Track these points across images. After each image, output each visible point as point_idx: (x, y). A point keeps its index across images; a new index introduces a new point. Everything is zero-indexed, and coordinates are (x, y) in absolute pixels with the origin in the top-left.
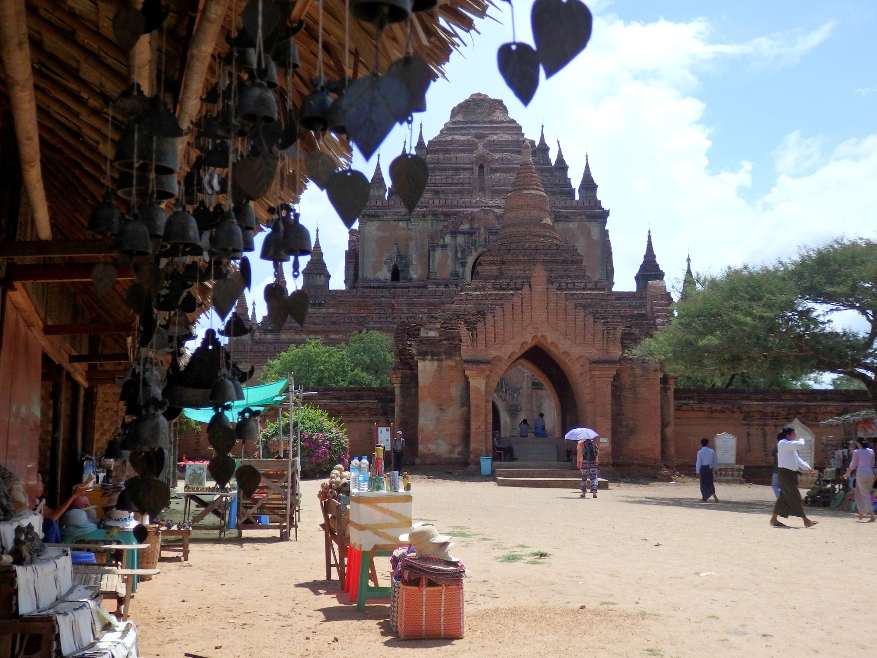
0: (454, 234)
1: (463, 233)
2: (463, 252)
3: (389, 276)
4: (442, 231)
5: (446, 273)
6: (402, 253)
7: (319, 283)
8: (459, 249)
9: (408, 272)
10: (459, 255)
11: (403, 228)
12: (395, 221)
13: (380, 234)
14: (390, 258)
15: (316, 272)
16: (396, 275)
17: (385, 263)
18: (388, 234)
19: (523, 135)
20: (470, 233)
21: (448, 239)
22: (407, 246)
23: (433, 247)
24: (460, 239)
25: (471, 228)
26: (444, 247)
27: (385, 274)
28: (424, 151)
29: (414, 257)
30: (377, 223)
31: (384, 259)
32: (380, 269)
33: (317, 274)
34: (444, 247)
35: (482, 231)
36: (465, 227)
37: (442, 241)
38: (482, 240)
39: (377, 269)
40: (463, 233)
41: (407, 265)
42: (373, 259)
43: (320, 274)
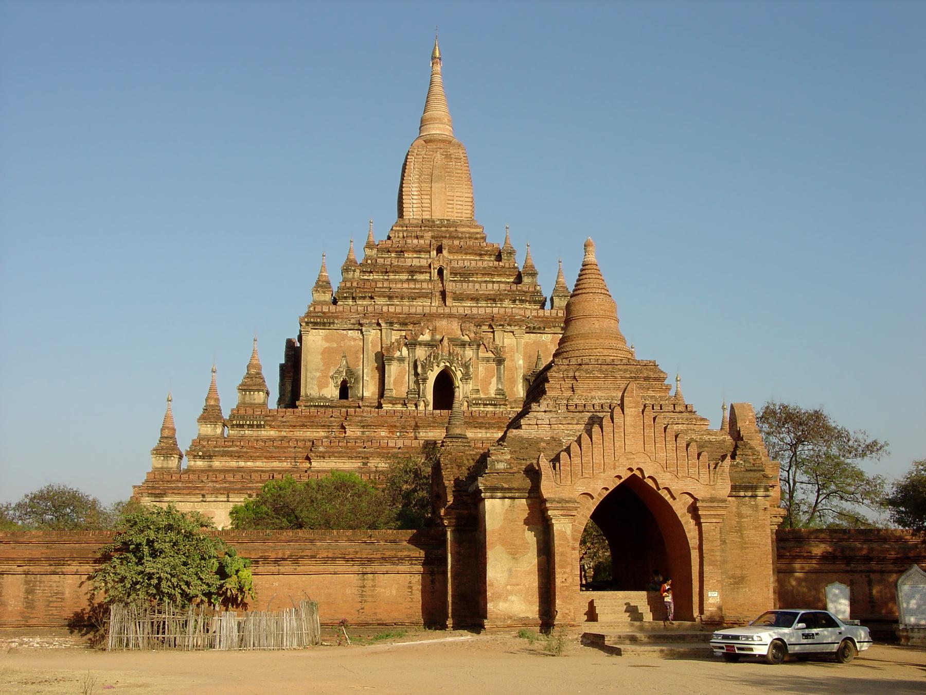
0: (412, 345)
2: (423, 367)
3: (336, 393)
4: (397, 340)
5: (402, 391)
6: (352, 367)
7: (256, 401)
8: (418, 363)
10: (419, 370)
13: (326, 345)
15: (254, 388)
16: (344, 391)
17: (332, 378)
19: (484, 238)
21: (405, 351)
24: (421, 353)
26: (401, 360)
27: (332, 392)
31: (331, 374)
32: (327, 385)
33: (254, 391)
34: (401, 360)
35: (445, 342)
36: (426, 337)
38: (446, 353)
39: (321, 386)
42: (318, 374)
43: (259, 391)
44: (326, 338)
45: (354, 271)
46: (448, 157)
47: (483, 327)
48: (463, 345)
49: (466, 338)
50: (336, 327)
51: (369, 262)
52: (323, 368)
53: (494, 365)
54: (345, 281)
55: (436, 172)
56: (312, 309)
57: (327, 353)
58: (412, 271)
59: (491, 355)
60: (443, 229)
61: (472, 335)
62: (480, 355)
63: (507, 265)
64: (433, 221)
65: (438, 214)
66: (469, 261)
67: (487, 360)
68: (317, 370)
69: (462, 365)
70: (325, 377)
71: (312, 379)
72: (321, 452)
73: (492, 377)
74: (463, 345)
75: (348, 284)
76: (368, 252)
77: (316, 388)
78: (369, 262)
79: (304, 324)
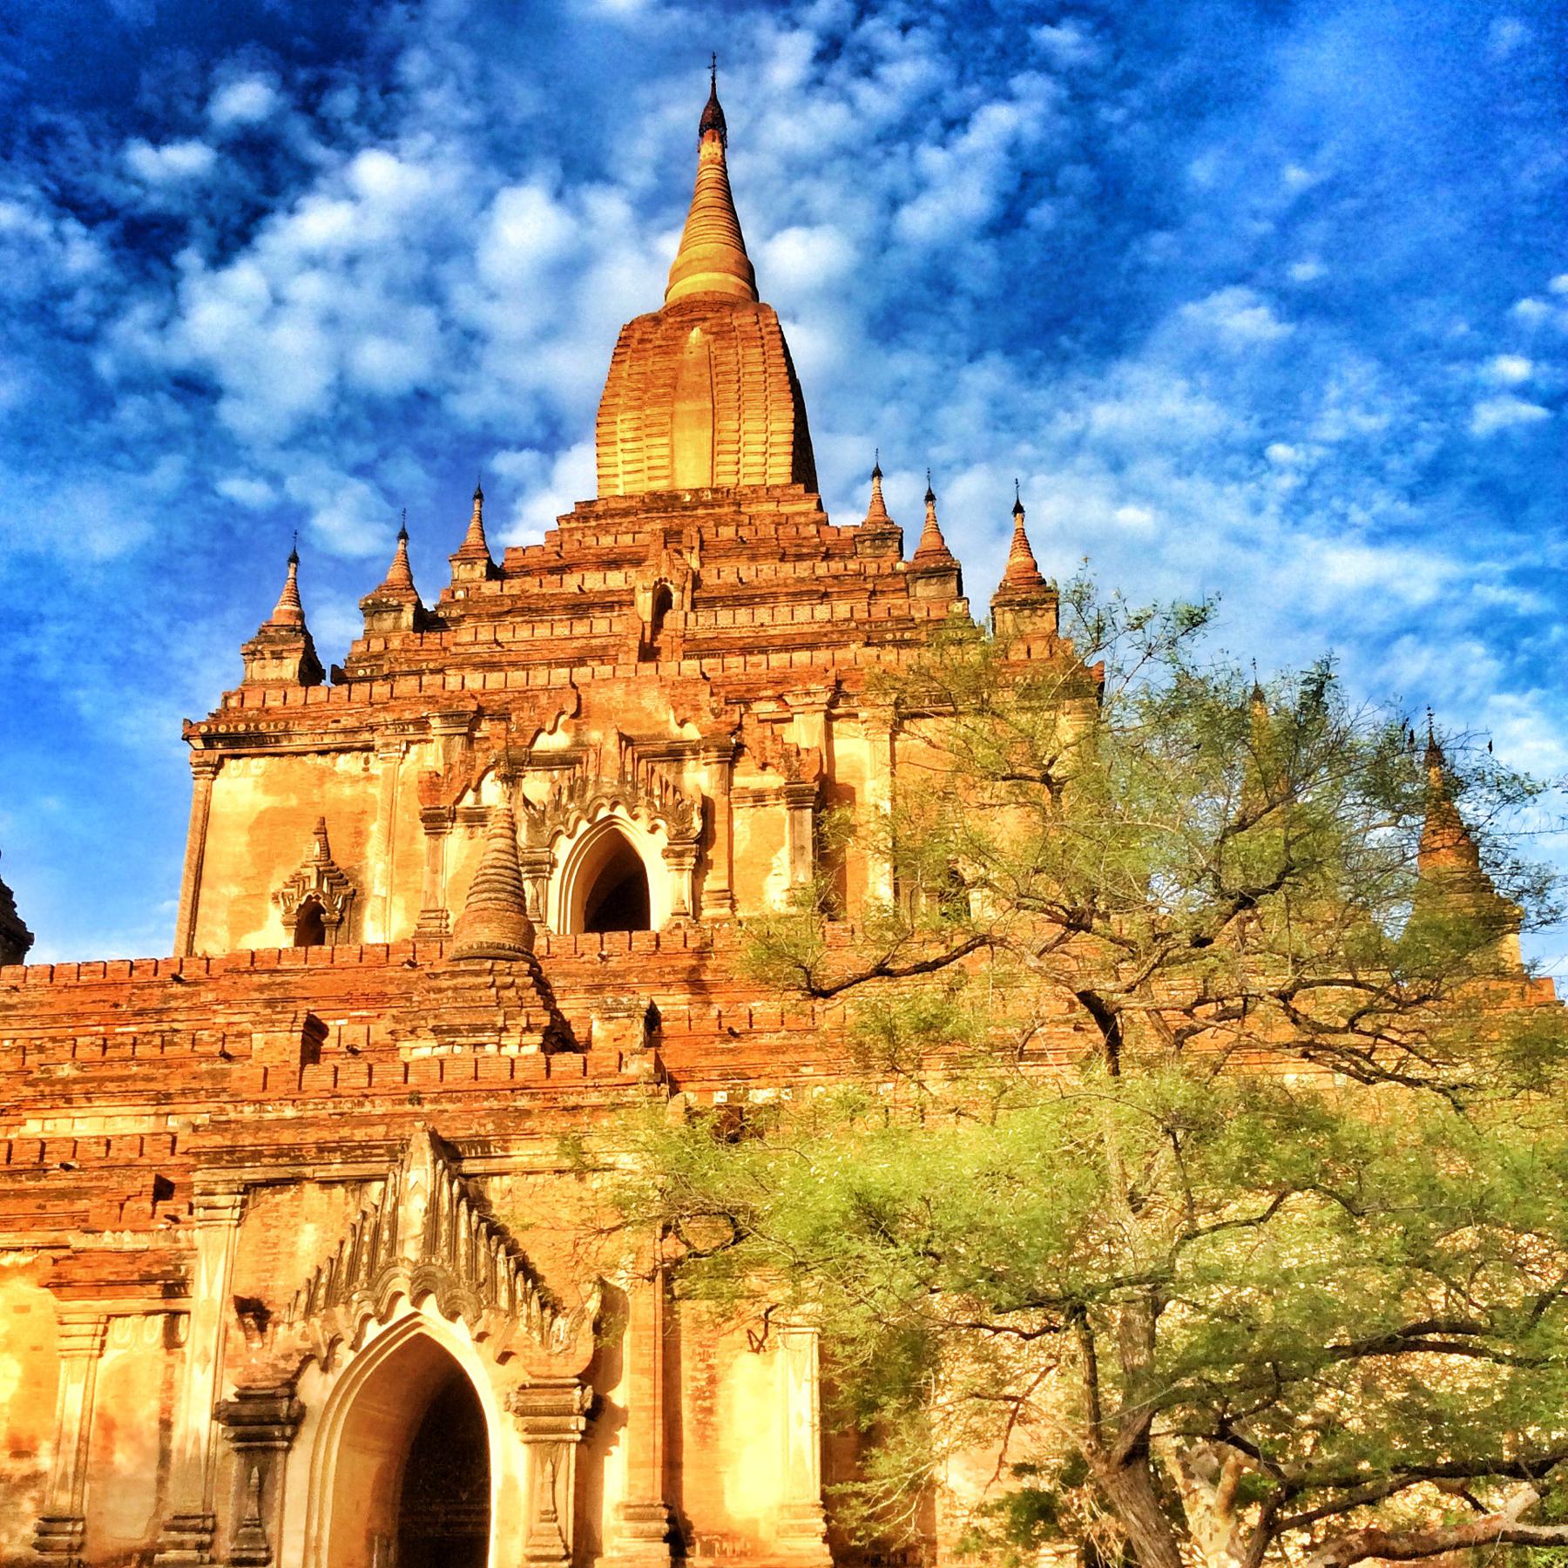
1: (549, 762)
2: (536, 824)
6: (341, 862)
9: (355, 928)
11: (354, 780)
12: (322, 753)
13: (265, 802)
14: (298, 880)
18: (293, 801)
20: (564, 761)
21: (493, 792)
22: (359, 836)
23: (435, 822)
25: (578, 743)
26: (477, 818)
28: (481, 568)
29: (376, 871)
30: (258, 765)
31: (276, 885)
32: (257, 922)
34: (477, 818)
37: (469, 799)
40: (549, 762)
41: (354, 901)
42: (234, 891)
44: (269, 784)
45: (399, 609)
46: (721, 334)
47: (757, 707)
48: (675, 754)
49: (691, 732)
50: (298, 743)
51: (460, 594)
52: (252, 872)
53: (782, 810)
54: (368, 636)
55: (689, 377)
56: (233, 703)
57: (266, 825)
58: (580, 607)
59: (773, 780)
60: (701, 512)
61: (708, 719)
62: (739, 781)
63: (872, 569)
64: (677, 497)
65: (691, 474)
66: (767, 571)
67: (759, 798)
68: (235, 877)
69: (664, 814)
70: (255, 897)
71: (213, 905)
72: (61, 1081)
73: (774, 849)
74: (675, 754)
75: (377, 646)
76: (463, 572)
77: (223, 933)
78: (460, 594)
79: (199, 744)
